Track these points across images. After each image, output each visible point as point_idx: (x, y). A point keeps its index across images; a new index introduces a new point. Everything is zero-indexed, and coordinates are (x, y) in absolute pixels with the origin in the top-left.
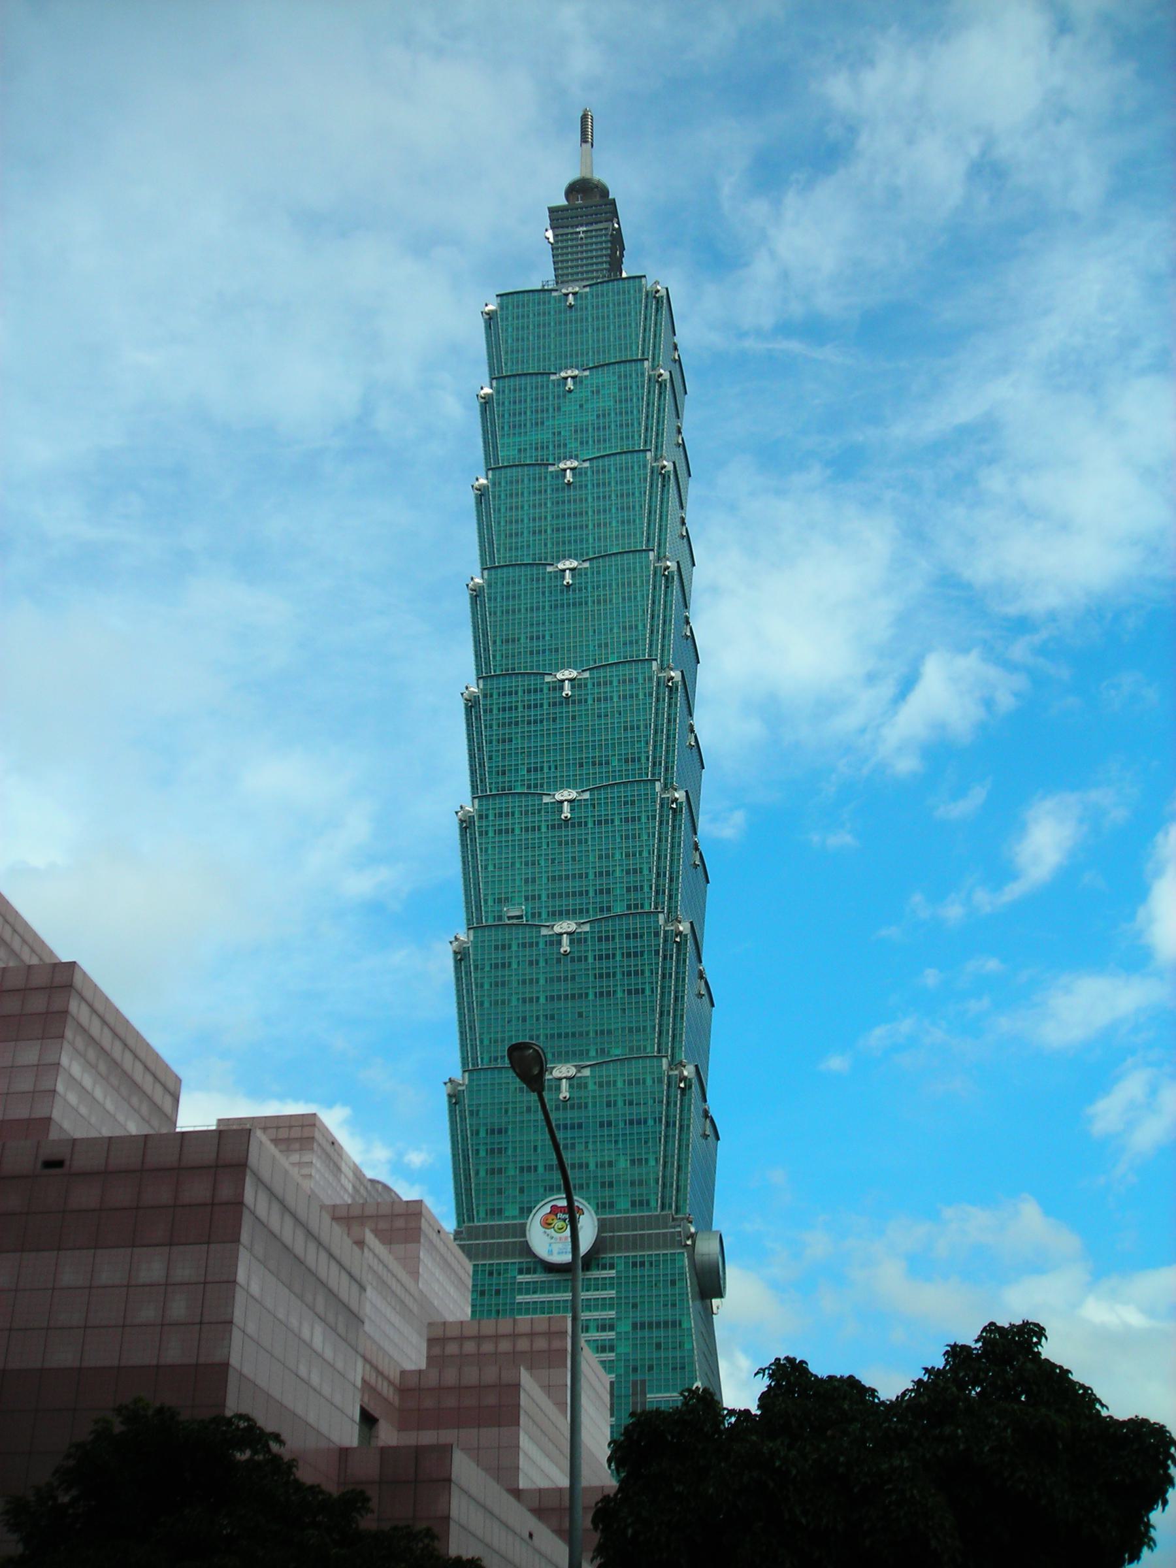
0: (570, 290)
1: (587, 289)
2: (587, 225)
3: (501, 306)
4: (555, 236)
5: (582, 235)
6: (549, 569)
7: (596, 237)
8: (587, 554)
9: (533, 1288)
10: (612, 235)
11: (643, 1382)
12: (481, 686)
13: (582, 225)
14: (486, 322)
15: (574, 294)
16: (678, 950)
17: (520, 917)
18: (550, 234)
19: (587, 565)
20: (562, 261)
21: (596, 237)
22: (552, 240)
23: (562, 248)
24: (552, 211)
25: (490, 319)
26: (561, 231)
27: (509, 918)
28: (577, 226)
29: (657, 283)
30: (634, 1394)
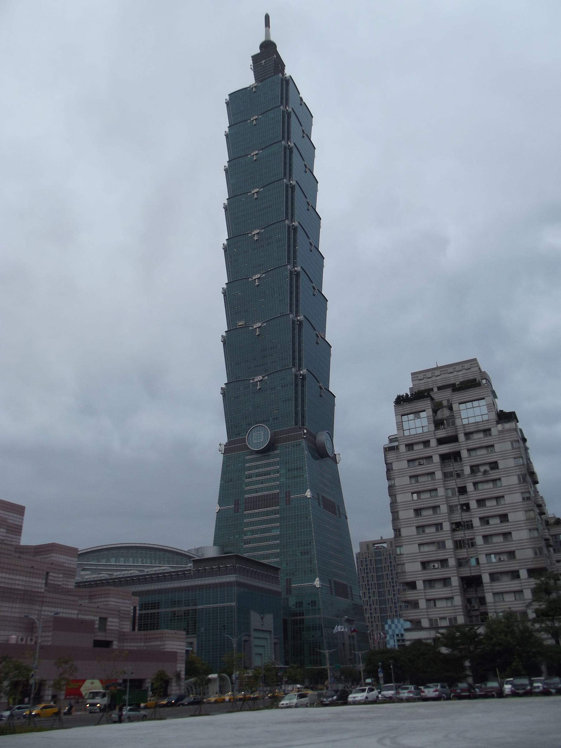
9: (252, 460)
11: (289, 491)
30: (286, 497)
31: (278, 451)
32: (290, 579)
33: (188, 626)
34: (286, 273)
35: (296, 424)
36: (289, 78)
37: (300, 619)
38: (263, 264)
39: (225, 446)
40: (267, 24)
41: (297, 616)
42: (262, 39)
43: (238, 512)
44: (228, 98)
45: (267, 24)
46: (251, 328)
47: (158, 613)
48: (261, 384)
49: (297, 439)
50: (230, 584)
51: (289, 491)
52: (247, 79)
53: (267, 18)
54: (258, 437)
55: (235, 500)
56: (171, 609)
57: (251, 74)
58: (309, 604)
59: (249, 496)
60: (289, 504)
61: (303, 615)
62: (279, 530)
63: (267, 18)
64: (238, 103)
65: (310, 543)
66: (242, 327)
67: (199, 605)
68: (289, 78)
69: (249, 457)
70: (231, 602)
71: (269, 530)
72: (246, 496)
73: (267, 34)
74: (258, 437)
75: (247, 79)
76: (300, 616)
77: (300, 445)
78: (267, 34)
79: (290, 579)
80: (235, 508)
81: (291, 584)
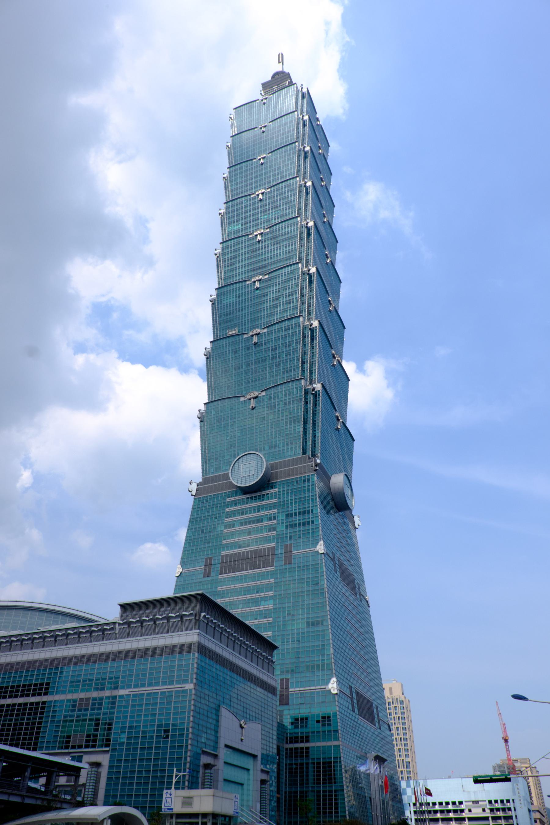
9: (236, 503)
11: (291, 545)
30: (286, 552)
31: (276, 490)
32: (288, 680)
33: (97, 730)
35: (304, 452)
37: (302, 748)
39: (198, 485)
41: (297, 742)
43: (209, 576)
47: (44, 703)
48: (256, 402)
49: (305, 473)
50: (185, 648)
51: (291, 545)
54: (248, 469)
55: (207, 559)
56: (69, 697)
58: (318, 722)
59: (227, 552)
60: (290, 563)
61: (307, 741)
62: (271, 602)
65: (322, 621)
67: (123, 688)
69: (232, 499)
70: (186, 681)
71: (258, 602)
72: (223, 553)
74: (248, 469)
76: (302, 742)
77: (309, 480)
79: (288, 680)
80: (205, 570)
81: (288, 688)
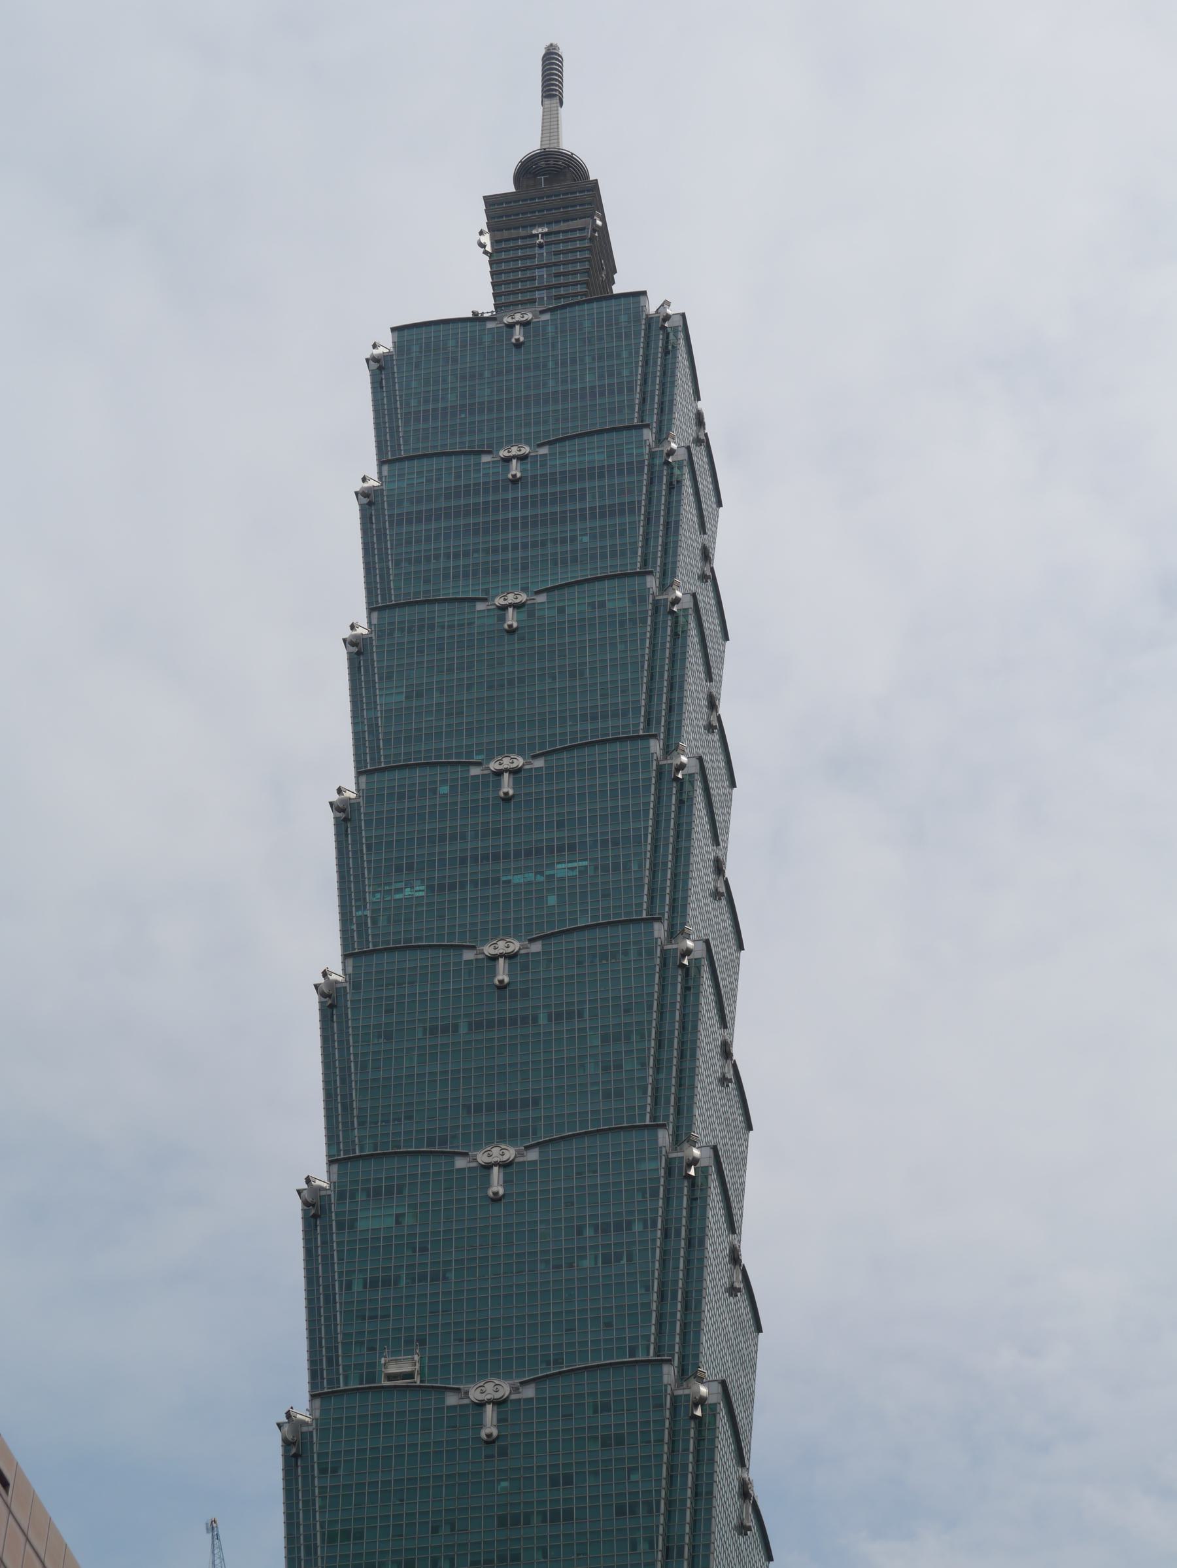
0: (518, 317)
1: (547, 317)
2: (549, 223)
3: (398, 345)
4: (495, 242)
5: (540, 240)
6: (475, 771)
7: (566, 241)
8: (542, 745)
10: (592, 239)
12: (350, 970)
13: (541, 225)
14: (373, 375)
15: (525, 324)
16: (699, 1432)
17: (410, 1375)
18: (486, 239)
19: (539, 763)
20: (506, 272)
21: (566, 241)
22: (489, 248)
23: (507, 261)
24: (492, 203)
25: (380, 368)
26: (506, 234)
27: (390, 1377)
28: (533, 226)
29: (666, 303)
34: (647, 1166)
36: (677, 322)
38: (536, 1102)
40: (552, 88)
42: (532, 144)
44: (387, 344)
45: (552, 88)
46: (452, 1400)
52: (460, 284)
53: (552, 62)
57: (481, 268)
63: (552, 62)
64: (417, 373)
66: (403, 1386)
68: (677, 322)
73: (551, 125)
75: (460, 284)
78: (551, 125)
